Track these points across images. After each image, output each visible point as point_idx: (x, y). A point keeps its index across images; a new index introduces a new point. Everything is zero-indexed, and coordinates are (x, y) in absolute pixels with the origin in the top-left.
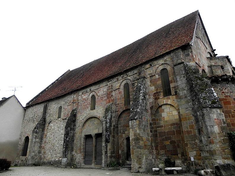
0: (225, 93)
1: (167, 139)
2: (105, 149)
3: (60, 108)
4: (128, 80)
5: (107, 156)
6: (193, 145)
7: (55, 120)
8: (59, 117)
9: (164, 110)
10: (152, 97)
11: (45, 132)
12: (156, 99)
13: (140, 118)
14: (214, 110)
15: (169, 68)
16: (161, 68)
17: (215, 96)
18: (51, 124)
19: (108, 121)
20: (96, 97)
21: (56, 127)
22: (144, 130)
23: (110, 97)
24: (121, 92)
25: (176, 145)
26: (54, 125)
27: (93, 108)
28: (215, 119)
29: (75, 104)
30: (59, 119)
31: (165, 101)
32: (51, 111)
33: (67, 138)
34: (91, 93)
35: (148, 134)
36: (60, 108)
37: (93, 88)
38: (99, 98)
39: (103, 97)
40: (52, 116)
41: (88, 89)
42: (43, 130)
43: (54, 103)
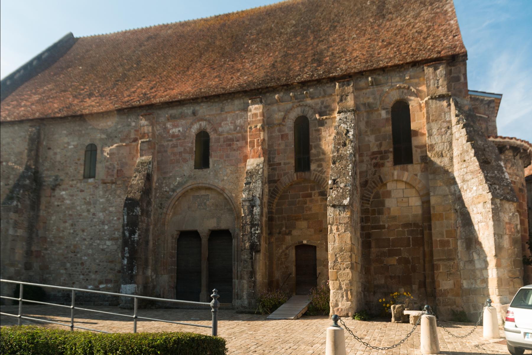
1: (391, 254)
2: (250, 267)
4: (307, 109)
5: (254, 282)
7: (75, 182)
8: (90, 174)
11: (42, 213)
20: (213, 136)
21: (78, 203)
25: (410, 267)
26: (72, 196)
28: (507, 223)
30: (91, 180)
32: (55, 154)
33: (132, 233)
38: (222, 140)
41: (188, 110)
42: (35, 205)
43: (65, 132)
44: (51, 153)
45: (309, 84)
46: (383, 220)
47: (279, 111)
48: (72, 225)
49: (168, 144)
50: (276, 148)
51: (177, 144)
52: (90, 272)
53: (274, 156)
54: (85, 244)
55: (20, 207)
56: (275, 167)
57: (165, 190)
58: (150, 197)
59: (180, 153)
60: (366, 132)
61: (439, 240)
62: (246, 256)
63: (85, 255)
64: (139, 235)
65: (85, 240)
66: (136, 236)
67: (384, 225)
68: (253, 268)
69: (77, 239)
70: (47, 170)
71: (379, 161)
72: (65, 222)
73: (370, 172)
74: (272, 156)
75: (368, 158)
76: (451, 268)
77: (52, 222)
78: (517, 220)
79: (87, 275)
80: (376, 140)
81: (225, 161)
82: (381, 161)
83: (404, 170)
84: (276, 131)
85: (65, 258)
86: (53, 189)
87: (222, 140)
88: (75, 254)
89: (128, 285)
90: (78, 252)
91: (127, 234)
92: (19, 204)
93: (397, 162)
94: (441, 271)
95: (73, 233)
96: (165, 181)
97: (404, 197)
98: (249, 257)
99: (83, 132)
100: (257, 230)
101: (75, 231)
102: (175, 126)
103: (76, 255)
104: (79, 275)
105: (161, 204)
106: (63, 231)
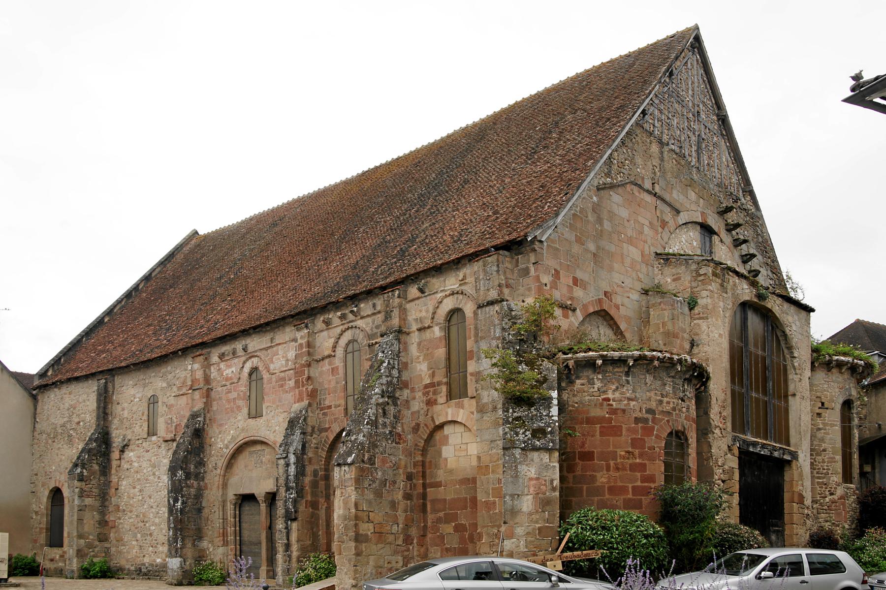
1: (448, 519)
2: (285, 538)
3: (153, 401)
4: (358, 331)
5: (290, 556)
6: (493, 539)
7: (140, 441)
9: (447, 437)
10: (419, 394)
11: (114, 479)
12: (430, 403)
14: (535, 455)
15: (469, 309)
16: (449, 304)
18: (130, 454)
20: (266, 376)
21: (145, 464)
23: (303, 382)
24: (337, 368)
26: (139, 457)
27: (255, 414)
28: (531, 479)
29: (197, 393)
30: (154, 438)
31: (450, 411)
33: (176, 500)
34: (247, 360)
35: (393, 505)
36: (153, 401)
37: (255, 343)
38: (274, 379)
39: (284, 379)
40: (127, 424)
41: (238, 345)
42: (105, 470)
43: (131, 382)
44: (119, 408)
45: (360, 297)
46: (441, 475)
47: (330, 337)
48: (140, 491)
49: (223, 390)
50: (326, 386)
51: (231, 389)
52: (157, 544)
53: (324, 397)
54: (152, 512)
55: (85, 474)
56: (326, 411)
57: (219, 446)
58: (202, 456)
59: (234, 399)
60: (418, 357)
61: (485, 501)
62: (281, 526)
63: (153, 525)
64: (183, 503)
65: (152, 507)
66: (179, 504)
67: (441, 482)
68: (288, 540)
69: (145, 507)
70: (117, 429)
71: (432, 396)
72: (134, 488)
73: (422, 412)
74: (322, 397)
75: (420, 394)
76: (495, 537)
77: (123, 488)
78: (555, 474)
79: (156, 547)
80: (430, 368)
81: (278, 406)
82: (434, 397)
83: (459, 407)
84: (327, 365)
85: (136, 528)
86: (122, 451)
87: (274, 379)
88: (144, 523)
89: (174, 559)
90: (147, 522)
91: (172, 502)
92: (84, 471)
93: (450, 396)
94: (483, 541)
95: (141, 500)
96: (220, 436)
97: (462, 443)
98: (284, 527)
99: (147, 381)
100: (292, 494)
101: (143, 498)
102: (229, 367)
103: (145, 525)
104: (149, 547)
105: (216, 464)
106: (133, 498)
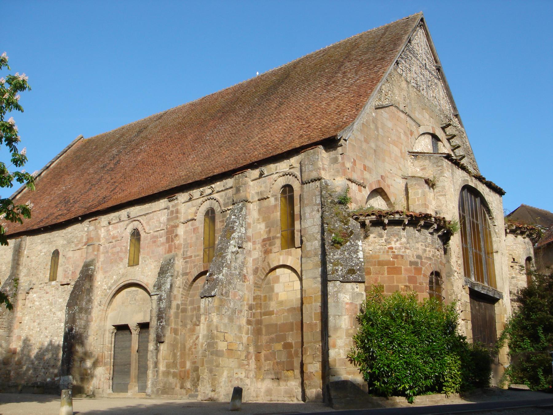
0: (394, 250)
3: (56, 254)
6: (316, 352)
7: (42, 285)
8: (53, 278)
9: (278, 278)
10: (258, 246)
12: (267, 252)
13: (222, 294)
15: (296, 185)
16: (282, 182)
17: (359, 258)
18: (33, 295)
19: (164, 295)
20: (143, 234)
21: (44, 303)
22: (231, 319)
23: (172, 238)
24: (198, 228)
25: (293, 352)
26: (40, 298)
27: (134, 262)
29: (90, 247)
30: (53, 283)
31: (281, 258)
32: (31, 261)
34: (130, 223)
35: (240, 328)
36: (56, 254)
37: (135, 210)
39: (156, 237)
40: (33, 272)
48: (39, 324)
49: (109, 245)
52: (49, 366)
57: (104, 288)
59: (118, 252)
65: (47, 337)
67: (273, 311)
69: (42, 336)
72: (34, 322)
77: (25, 322)
79: (47, 369)
80: (266, 227)
83: (288, 255)
84: (190, 226)
97: (290, 282)
101: (40, 330)
105: (101, 302)
106: (32, 330)
